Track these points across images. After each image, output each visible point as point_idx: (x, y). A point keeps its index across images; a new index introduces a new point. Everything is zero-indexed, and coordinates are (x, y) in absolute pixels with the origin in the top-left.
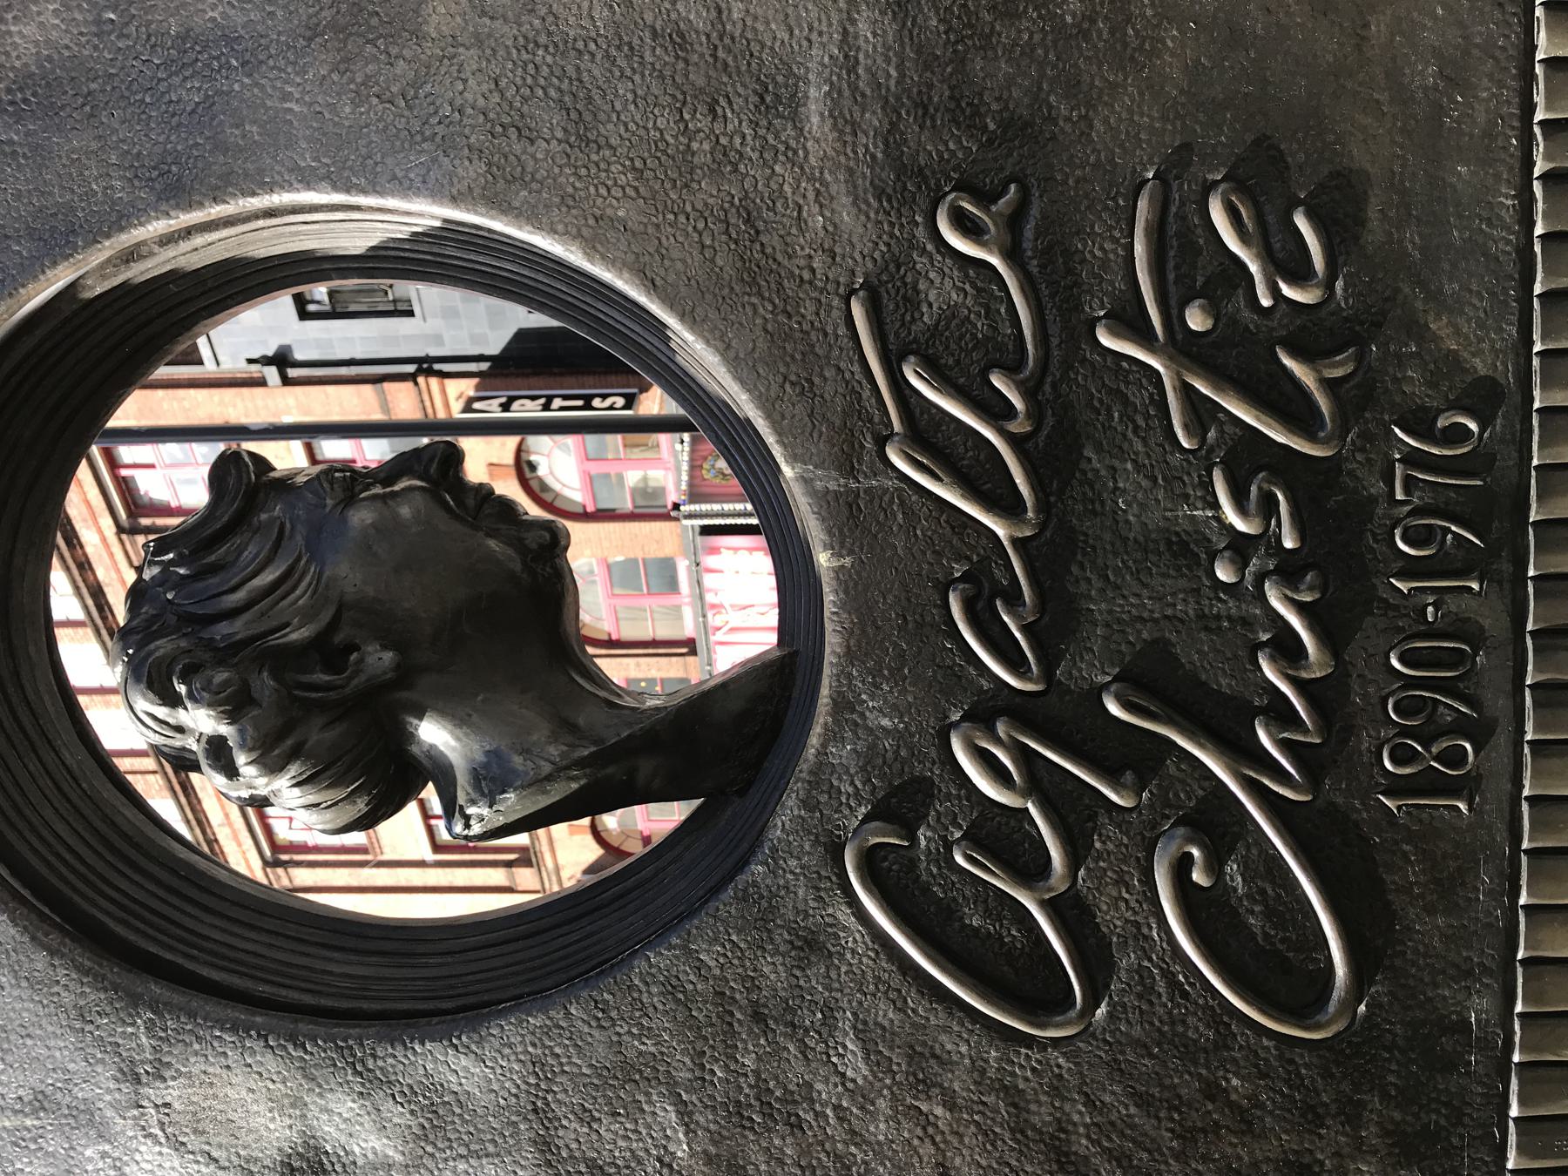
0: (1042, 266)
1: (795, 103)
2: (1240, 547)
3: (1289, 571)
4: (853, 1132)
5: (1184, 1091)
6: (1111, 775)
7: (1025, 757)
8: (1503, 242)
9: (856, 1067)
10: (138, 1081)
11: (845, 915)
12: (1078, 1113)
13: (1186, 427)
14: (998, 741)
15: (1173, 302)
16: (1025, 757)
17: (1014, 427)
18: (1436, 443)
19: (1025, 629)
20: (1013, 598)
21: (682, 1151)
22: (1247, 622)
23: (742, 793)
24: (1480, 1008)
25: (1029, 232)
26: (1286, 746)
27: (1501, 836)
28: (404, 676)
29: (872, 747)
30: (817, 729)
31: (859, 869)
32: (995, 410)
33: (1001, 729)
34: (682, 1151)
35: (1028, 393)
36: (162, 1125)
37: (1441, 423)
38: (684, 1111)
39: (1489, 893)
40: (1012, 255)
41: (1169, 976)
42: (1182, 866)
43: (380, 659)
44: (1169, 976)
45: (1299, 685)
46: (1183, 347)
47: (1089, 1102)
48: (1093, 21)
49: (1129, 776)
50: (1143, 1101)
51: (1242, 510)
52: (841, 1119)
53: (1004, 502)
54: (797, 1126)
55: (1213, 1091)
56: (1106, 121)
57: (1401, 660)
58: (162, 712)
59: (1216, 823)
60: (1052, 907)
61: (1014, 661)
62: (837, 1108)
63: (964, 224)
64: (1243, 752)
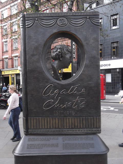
7: (57, 93)
16: (57, 93)
20: (65, 93)
26: (58, 106)
28: (60, 60)
32: (74, 92)
40: (82, 92)
42: (52, 101)
43: (61, 59)
46: (77, 101)
53: (70, 92)
58: (59, 48)
59: (54, 103)
60: (49, 95)
61: (62, 93)
63: (84, 90)
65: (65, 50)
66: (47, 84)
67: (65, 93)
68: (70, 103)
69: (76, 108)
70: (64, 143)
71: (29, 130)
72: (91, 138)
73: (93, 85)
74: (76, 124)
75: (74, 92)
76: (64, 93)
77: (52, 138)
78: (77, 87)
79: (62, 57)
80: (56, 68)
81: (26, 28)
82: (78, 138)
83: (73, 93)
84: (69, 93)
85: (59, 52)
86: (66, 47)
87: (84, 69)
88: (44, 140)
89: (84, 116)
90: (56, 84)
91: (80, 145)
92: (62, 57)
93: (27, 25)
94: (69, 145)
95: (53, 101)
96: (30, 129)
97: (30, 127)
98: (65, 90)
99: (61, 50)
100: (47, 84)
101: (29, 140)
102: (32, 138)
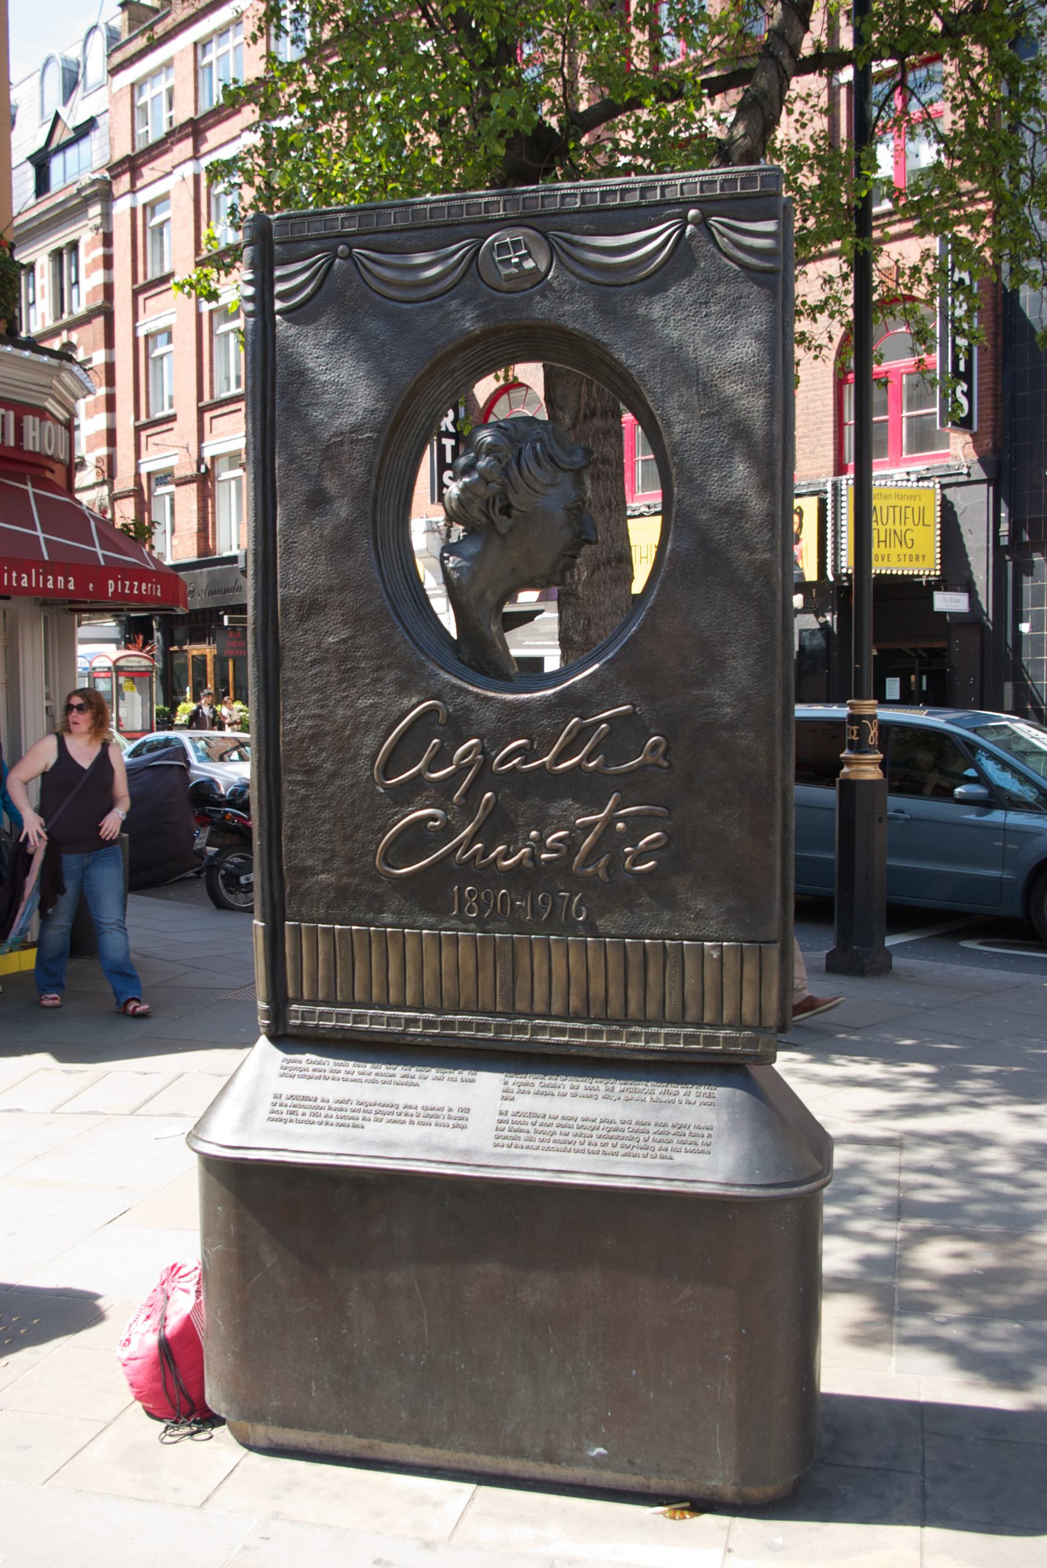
2: (541, 840)
3: (533, 857)
4: (339, 702)
5: (357, 818)
6: (465, 795)
7: (469, 767)
8: (643, 929)
9: (362, 703)
10: (352, 433)
11: (414, 700)
12: (348, 782)
13: (583, 822)
14: (475, 756)
16: (469, 767)
18: (577, 907)
19: (514, 766)
21: (331, 640)
22: (516, 842)
23: (459, 659)
24: (388, 917)
26: (474, 856)
27: (445, 925)
29: (473, 711)
30: (480, 691)
31: (430, 705)
33: (480, 757)
34: (331, 640)
36: (335, 442)
37: (583, 908)
38: (344, 641)
39: (426, 921)
41: (396, 814)
42: (434, 818)
45: (495, 859)
46: (610, 822)
47: (352, 786)
49: (463, 801)
50: (353, 803)
51: (554, 841)
52: (343, 697)
54: (341, 682)
55: (357, 828)
57: (504, 894)
59: (448, 831)
61: (503, 762)
62: (347, 696)
64: (473, 839)
66: (406, 703)
68: (559, 840)
70: (510, 1107)
73: (729, 710)
74: (597, 987)
75: (589, 758)
86: (541, 440)
87: (658, 595)
88: (380, 1079)
89: (657, 931)
91: (616, 1130)
93: (284, 296)
94: (540, 1120)
100: (406, 703)
101: (286, 1073)
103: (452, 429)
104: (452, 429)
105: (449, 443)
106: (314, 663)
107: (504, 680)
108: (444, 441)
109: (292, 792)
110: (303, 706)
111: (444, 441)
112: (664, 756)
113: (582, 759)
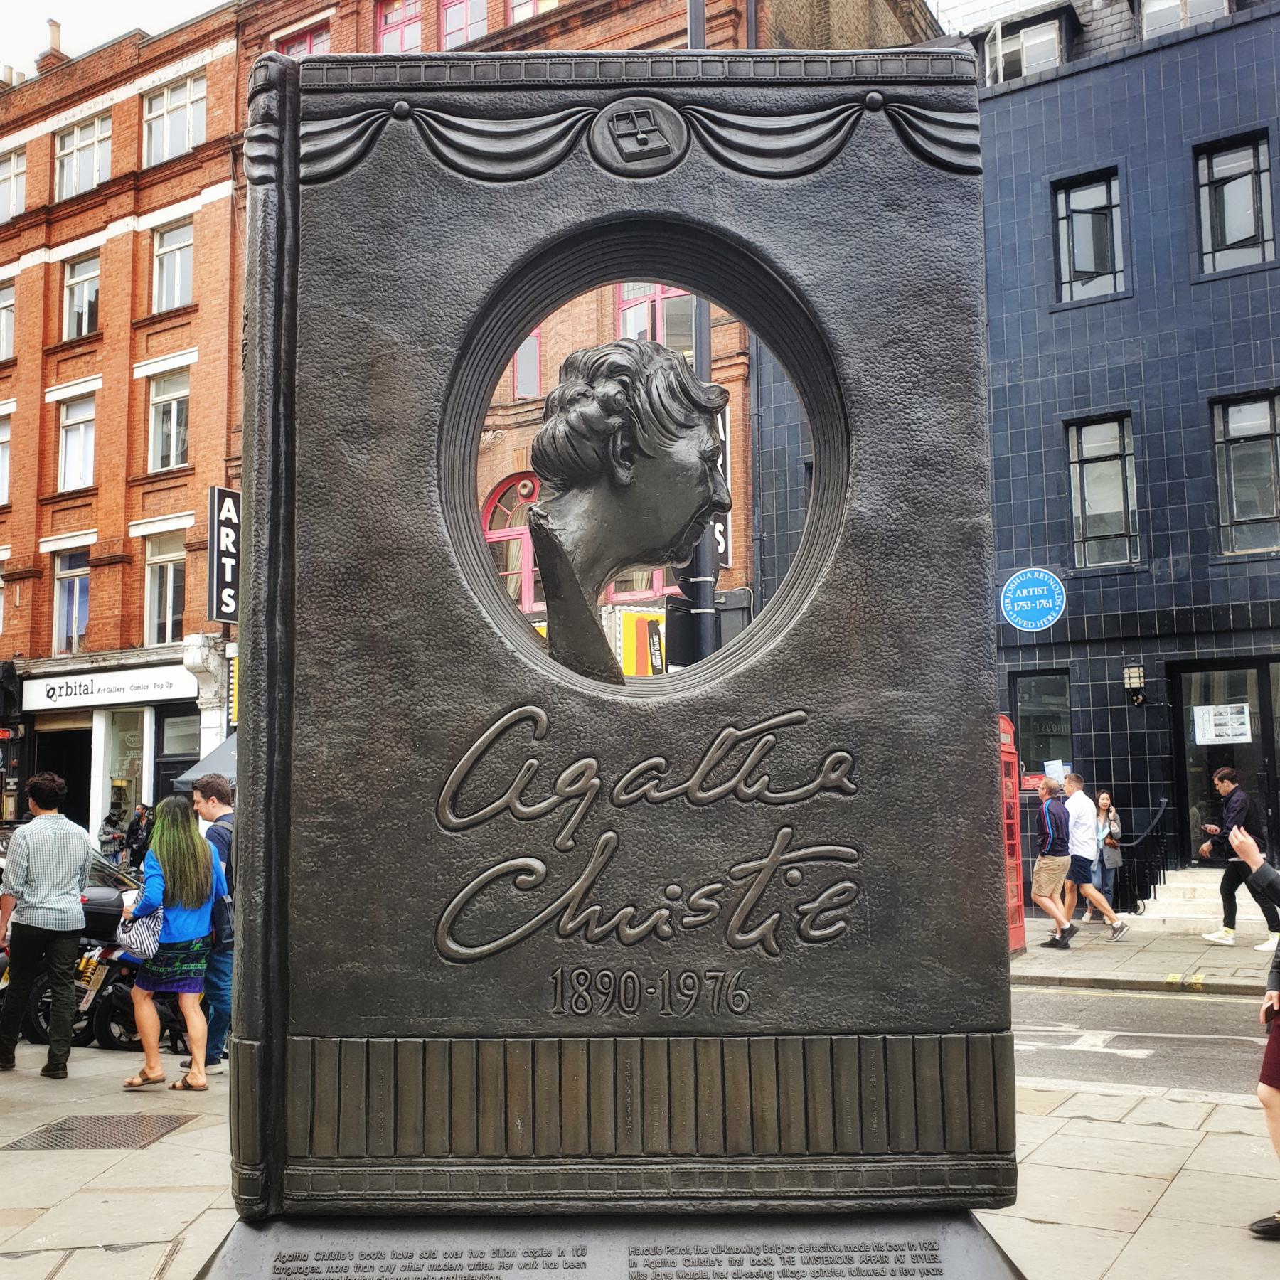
0: (816, 802)
1: (896, 685)
7: (581, 795)
11: (497, 707)
15: (801, 864)
17: (742, 786)
23: (551, 656)
25: (832, 795)
26: (586, 923)
35: (758, 797)
40: (823, 788)
41: (468, 867)
42: (529, 871)
44: (468, 867)
46: (779, 870)
48: (932, 826)
56: (886, 832)
60: (508, 807)
61: (626, 790)
65: (659, 384)
67: (655, 795)
68: (708, 896)
69: (762, 941)
71: (292, 1170)
72: (915, 1259)
75: (748, 781)
76: (644, 795)
77: (520, 1259)
78: (771, 737)
79: (627, 454)
80: (578, 559)
81: (301, 188)
82: (786, 1249)
83: (734, 791)
84: (700, 795)
85: (607, 405)
90: (576, 707)
92: (627, 454)
95: (537, 864)
96: (299, 1160)
97: (297, 1145)
98: (656, 767)
99: (622, 383)
102: (320, 1256)
103: (232, 550)
104: (232, 550)
105: (229, 562)
106: (352, 655)
107: (614, 683)
108: (224, 560)
109: (311, 842)
110: (329, 715)
111: (224, 560)
112: (849, 774)
113: (739, 782)
